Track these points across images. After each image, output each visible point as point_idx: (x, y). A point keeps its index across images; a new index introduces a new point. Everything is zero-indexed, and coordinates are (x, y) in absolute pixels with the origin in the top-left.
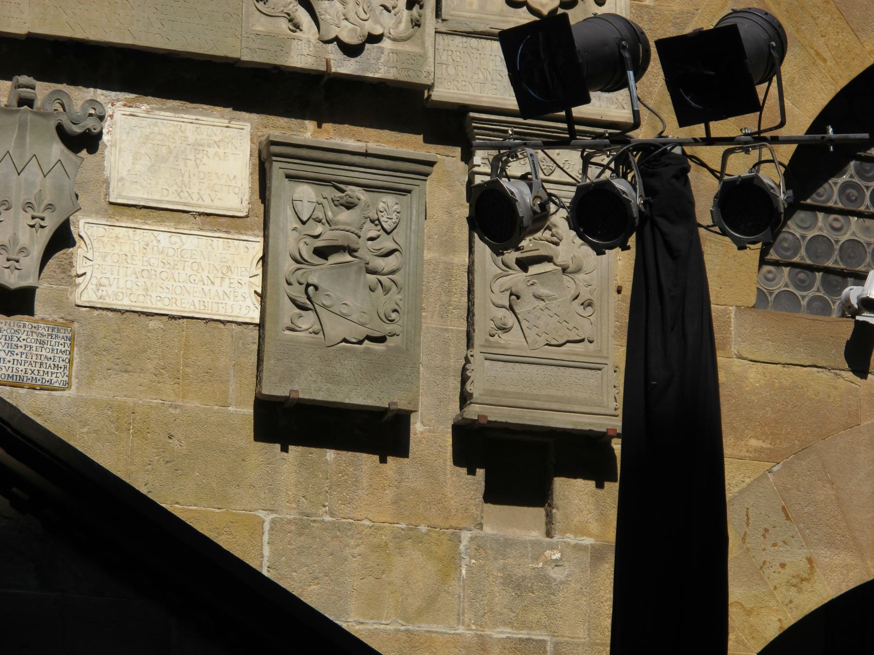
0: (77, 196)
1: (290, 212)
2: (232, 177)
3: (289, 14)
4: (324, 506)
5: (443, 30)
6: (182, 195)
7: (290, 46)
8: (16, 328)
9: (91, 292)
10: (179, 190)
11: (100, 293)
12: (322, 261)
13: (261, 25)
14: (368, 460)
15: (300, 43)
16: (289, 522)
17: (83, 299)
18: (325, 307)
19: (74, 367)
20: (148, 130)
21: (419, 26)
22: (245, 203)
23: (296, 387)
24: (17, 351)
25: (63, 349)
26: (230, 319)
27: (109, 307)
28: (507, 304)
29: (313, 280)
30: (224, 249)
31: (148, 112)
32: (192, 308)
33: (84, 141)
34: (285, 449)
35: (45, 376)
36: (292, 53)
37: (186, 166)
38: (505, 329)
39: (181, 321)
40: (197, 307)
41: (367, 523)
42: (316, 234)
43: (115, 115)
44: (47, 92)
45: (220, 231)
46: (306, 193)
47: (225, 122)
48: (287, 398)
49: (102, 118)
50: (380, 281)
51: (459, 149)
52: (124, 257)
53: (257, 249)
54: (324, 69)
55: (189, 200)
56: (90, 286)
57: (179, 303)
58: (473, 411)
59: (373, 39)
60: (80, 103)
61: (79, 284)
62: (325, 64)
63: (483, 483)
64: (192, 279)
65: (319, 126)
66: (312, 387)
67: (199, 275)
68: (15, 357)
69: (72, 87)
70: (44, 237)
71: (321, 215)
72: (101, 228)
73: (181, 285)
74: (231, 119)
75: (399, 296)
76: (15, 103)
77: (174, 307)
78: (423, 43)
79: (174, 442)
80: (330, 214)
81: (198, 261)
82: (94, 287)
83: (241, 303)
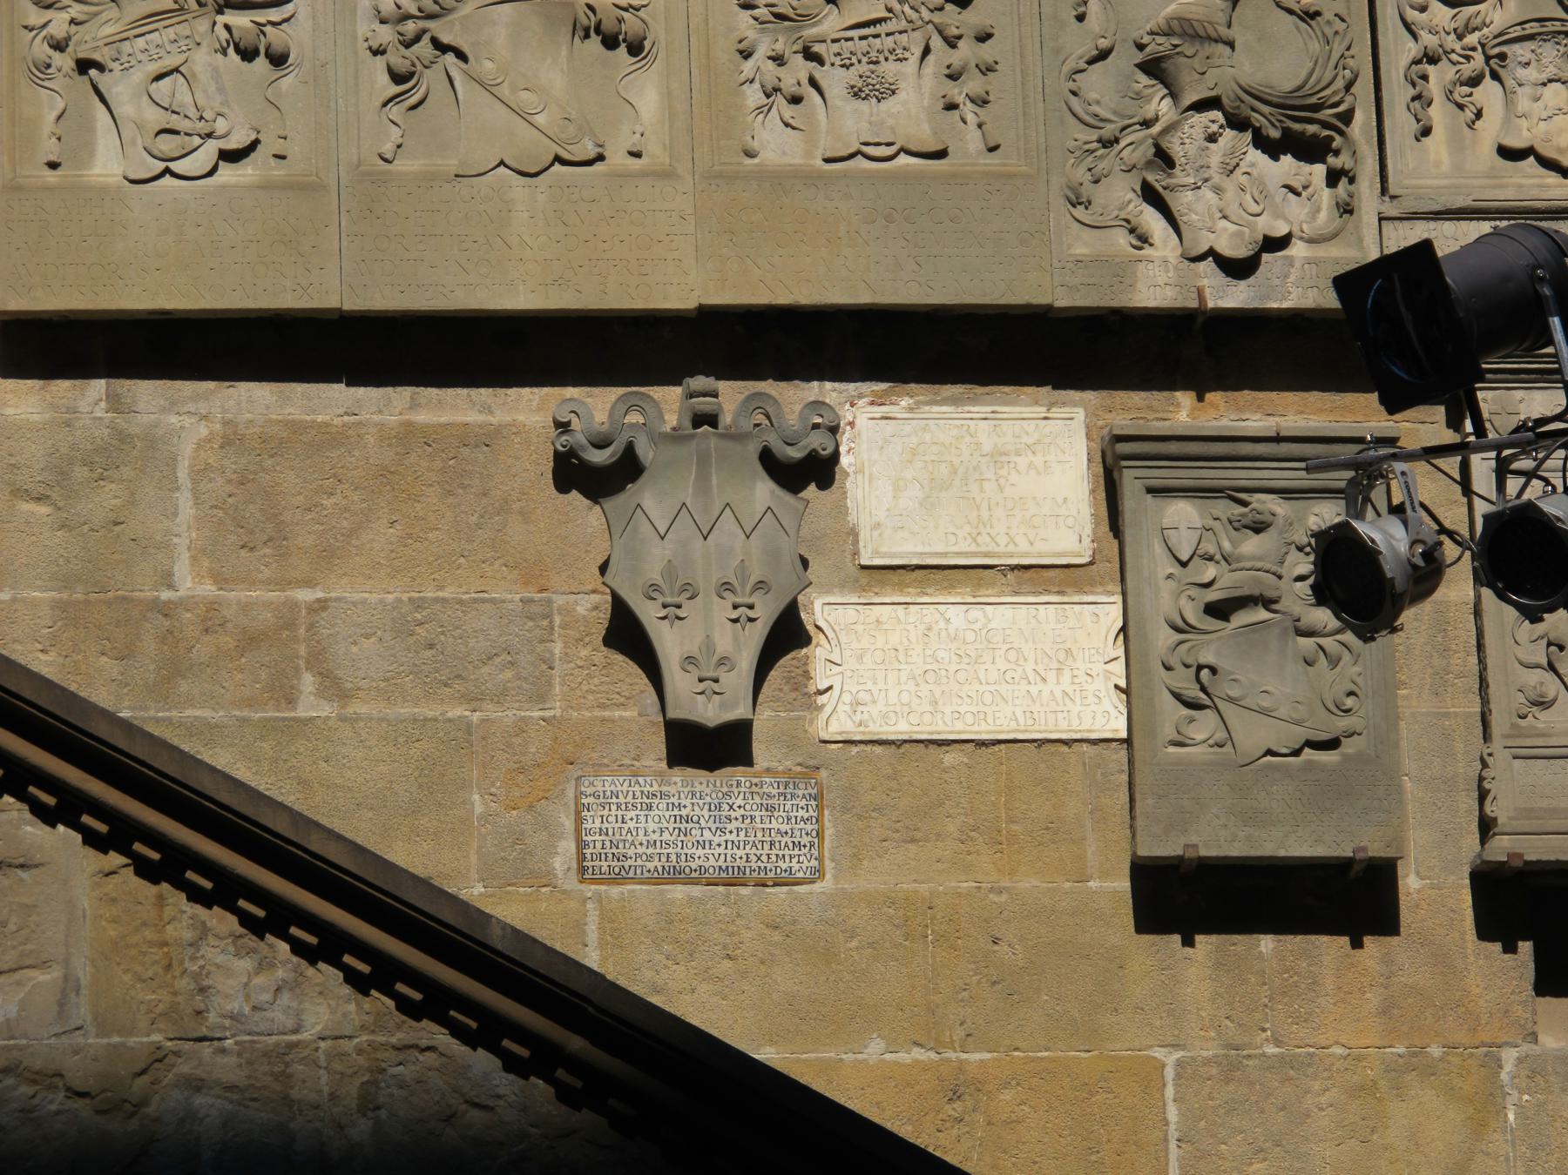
0: (805, 563)
1: (1159, 549)
2: (1060, 501)
3: (1128, 221)
4: (1264, 1030)
5: (1395, 213)
6: (979, 539)
7: (1134, 274)
8: (725, 790)
9: (842, 716)
10: (975, 533)
11: (858, 718)
12: (1220, 624)
13: (1083, 244)
14: (1332, 947)
15: (1150, 266)
16: (1207, 1062)
17: (831, 729)
18: (1231, 700)
19: (827, 844)
20: (915, 440)
21: (1351, 212)
22: (1087, 541)
23: (1194, 839)
24: (729, 827)
25: (806, 816)
26: (1078, 736)
27: (875, 738)
28: (1544, 662)
29: (1207, 657)
30: (1058, 622)
31: (911, 410)
32: (1013, 725)
33: (811, 471)
34: (1188, 942)
35: (780, 863)
36: (1139, 286)
37: (982, 490)
38: (1543, 704)
39: (996, 748)
40: (1022, 721)
41: (1338, 1050)
42: (1206, 580)
43: (858, 422)
44: (742, 397)
45: (1048, 592)
46: (1183, 514)
47: (1041, 411)
48: (1181, 858)
49: (834, 430)
50: (1321, 647)
51: (1442, 409)
52: (893, 653)
53: (1112, 615)
54: (1194, 304)
55: (992, 548)
56: (841, 707)
57: (990, 721)
58: (1501, 848)
59: (1274, 244)
60: (798, 408)
61: (823, 706)
62: (1195, 295)
63: (1532, 965)
64: (1008, 676)
65: (1200, 399)
66: (1219, 836)
67: (1020, 670)
68: (728, 837)
69: (783, 384)
70: (755, 636)
71: (1211, 548)
72: (851, 610)
73: (992, 688)
74: (1050, 406)
75: (1357, 669)
76: (688, 423)
77: (984, 727)
78: (1360, 240)
79: (1003, 948)
80: (1227, 545)
81: (1016, 645)
82: (847, 708)
83: (1094, 707)
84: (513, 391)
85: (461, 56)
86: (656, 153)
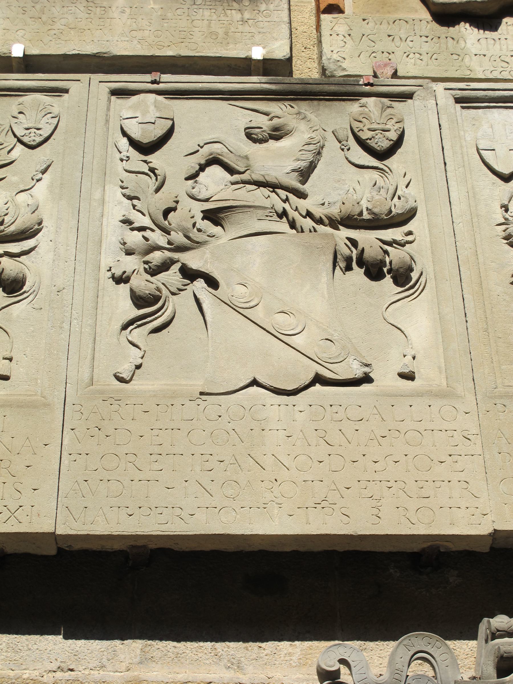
76: (491, 670)
84: (269, 646)
85: (212, 283)
86: (428, 375)
